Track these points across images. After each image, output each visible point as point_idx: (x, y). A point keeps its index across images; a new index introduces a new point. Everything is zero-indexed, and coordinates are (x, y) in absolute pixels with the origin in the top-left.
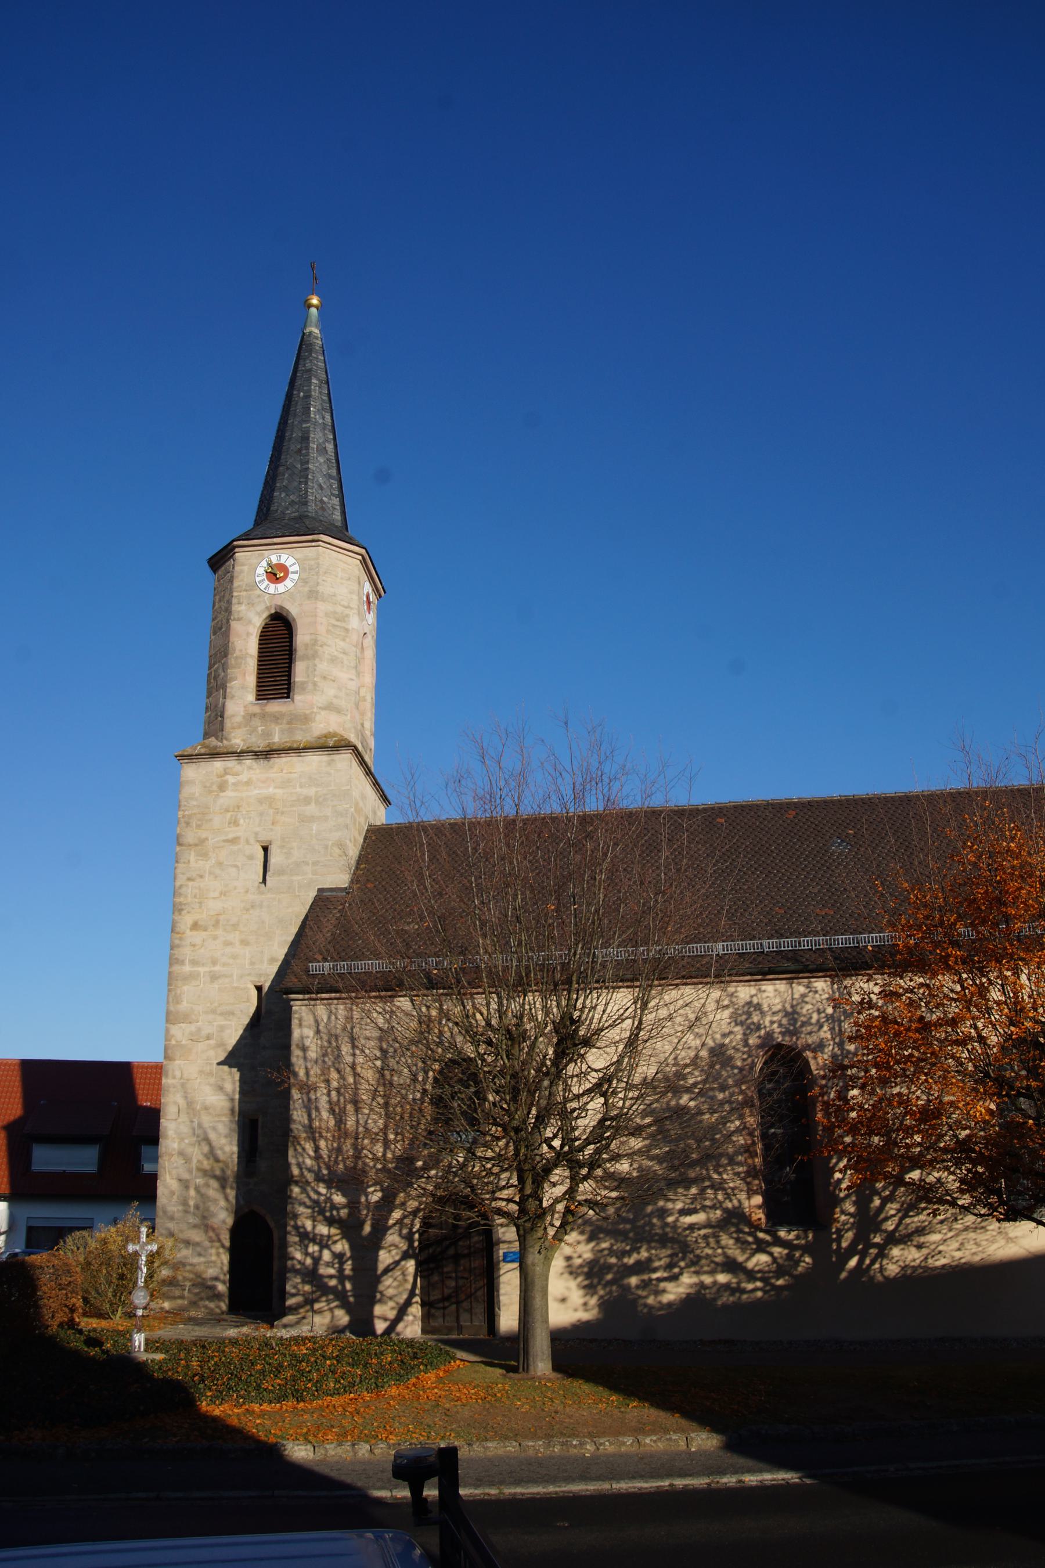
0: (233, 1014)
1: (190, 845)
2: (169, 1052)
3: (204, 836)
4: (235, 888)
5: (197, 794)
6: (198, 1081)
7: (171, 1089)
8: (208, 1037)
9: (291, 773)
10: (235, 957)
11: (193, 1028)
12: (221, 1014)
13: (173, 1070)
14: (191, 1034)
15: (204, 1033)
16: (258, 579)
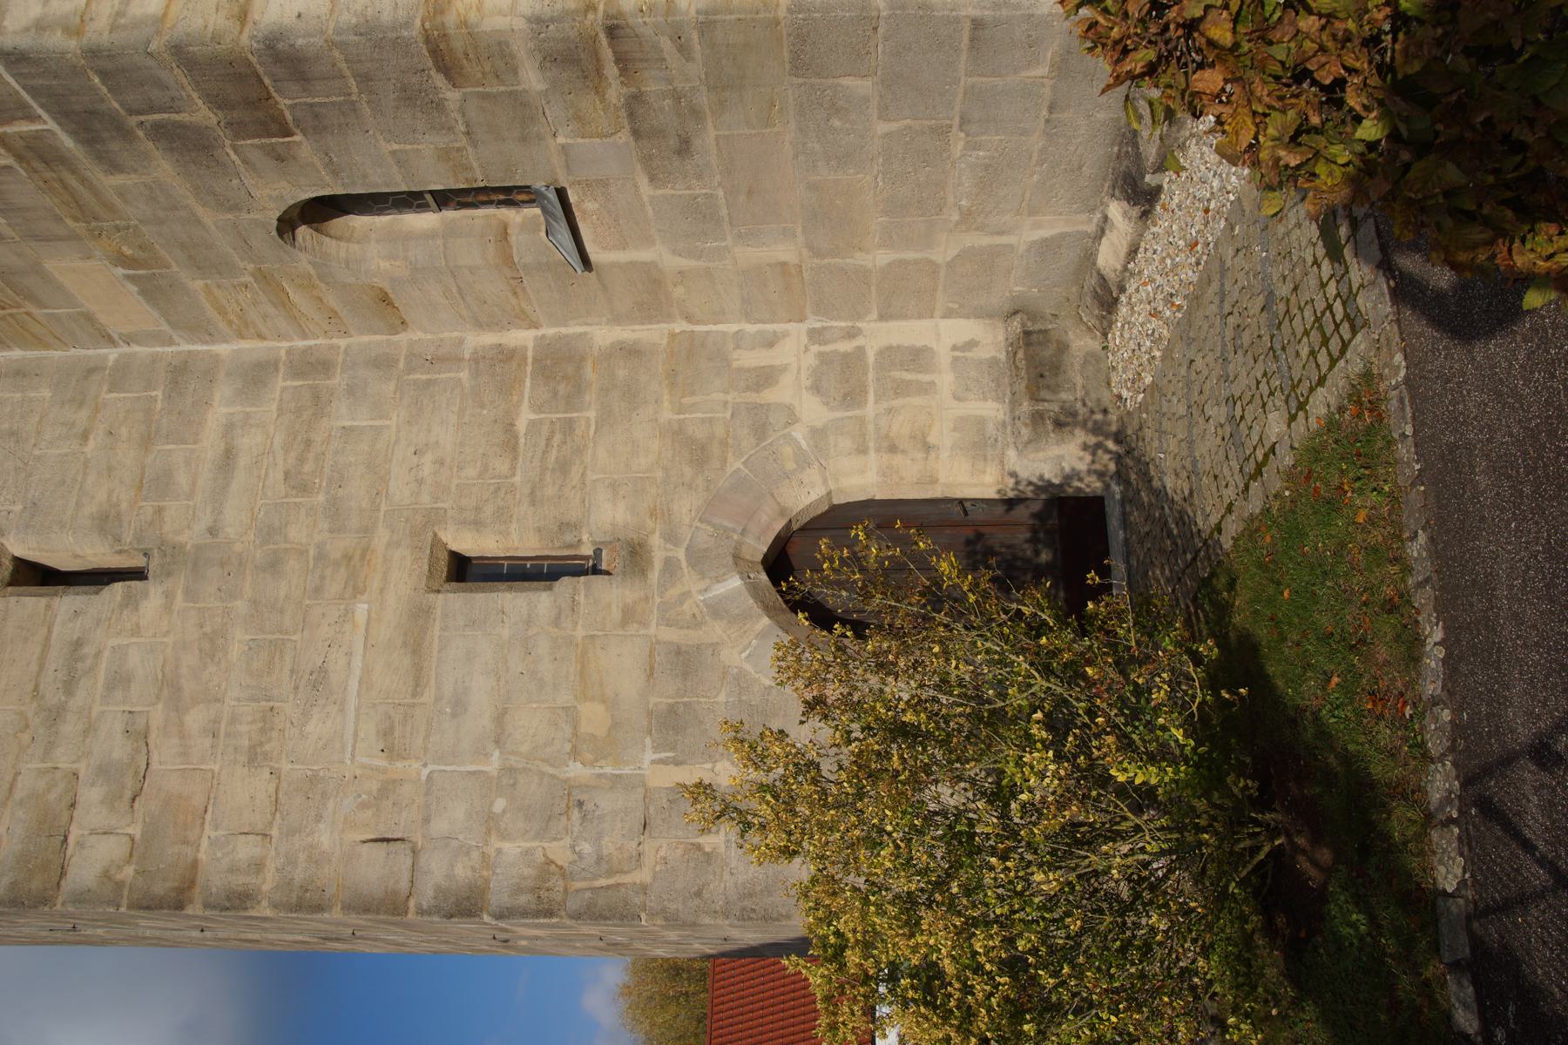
0: (78, 644)
2: (160, 888)
6: (286, 766)
7: (299, 875)
8: (139, 736)
11: (91, 795)
12: (69, 686)
13: (233, 870)
14: (110, 801)
15: (119, 749)
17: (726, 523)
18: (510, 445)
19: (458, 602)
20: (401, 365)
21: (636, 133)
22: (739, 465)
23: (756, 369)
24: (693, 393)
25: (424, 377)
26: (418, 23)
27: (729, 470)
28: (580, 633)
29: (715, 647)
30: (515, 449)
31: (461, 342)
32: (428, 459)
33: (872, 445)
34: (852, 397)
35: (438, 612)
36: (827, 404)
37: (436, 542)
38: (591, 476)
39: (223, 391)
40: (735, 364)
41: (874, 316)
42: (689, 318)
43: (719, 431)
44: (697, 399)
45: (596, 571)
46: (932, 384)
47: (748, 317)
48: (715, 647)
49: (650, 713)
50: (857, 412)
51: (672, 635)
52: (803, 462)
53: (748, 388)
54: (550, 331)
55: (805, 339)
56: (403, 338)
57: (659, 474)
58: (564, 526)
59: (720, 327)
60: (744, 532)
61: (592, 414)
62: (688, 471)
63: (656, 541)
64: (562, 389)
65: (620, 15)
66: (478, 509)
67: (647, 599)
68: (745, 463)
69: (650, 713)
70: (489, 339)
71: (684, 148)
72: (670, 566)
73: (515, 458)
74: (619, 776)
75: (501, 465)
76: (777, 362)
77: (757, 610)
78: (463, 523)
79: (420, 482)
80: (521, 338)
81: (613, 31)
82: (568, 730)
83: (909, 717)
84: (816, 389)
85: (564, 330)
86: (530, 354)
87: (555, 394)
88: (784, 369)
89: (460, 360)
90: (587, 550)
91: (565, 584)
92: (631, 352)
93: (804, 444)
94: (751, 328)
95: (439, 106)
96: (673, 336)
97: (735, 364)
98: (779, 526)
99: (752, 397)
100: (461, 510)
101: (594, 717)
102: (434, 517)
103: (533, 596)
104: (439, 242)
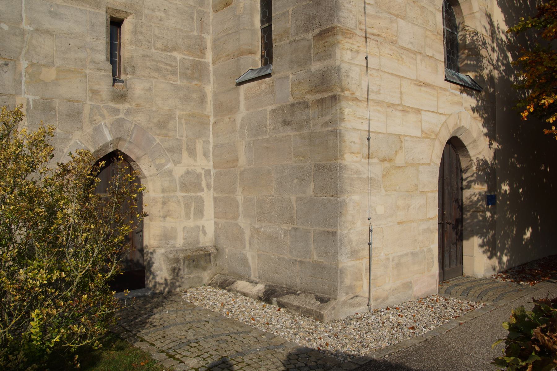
17: (134, 135)
18: (167, 49)
19: (102, 20)
20: (200, 8)
21: (293, 105)
22: (158, 141)
23: (195, 149)
24: (186, 123)
25: (195, 17)
26: (339, 25)
27: (156, 137)
28: (88, 71)
29: (81, 129)
30: (165, 50)
31: (208, 33)
32: (162, 14)
33: (166, 195)
34: (185, 187)
35: (97, 11)
36: (182, 177)
37: (128, 14)
38: (154, 81)
40: (197, 141)
41: (216, 195)
42: (215, 123)
43: (171, 134)
44: (184, 125)
45: (114, 80)
46: (190, 218)
47: (215, 146)
48: (81, 129)
49: (51, 99)
50: (178, 188)
51: (86, 110)
52: (159, 167)
53: (188, 146)
54: (211, 69)
55: (206, 168)
56: (210, 10)
57: (154, 109)
58: (134, 68)
59: (211, 136)
60: (130, 142)
61: (179, 83)
62: (155, 120)
63: (127, 106)
64: (189, 72)
65: (340, 101)
66: (141, 33)
67: (102, 101)
68: (158, 144)
69: (51, 99)
70: (209, 44)
71: (286, 123)
72: (116, 111)
73: (162, 50)
74: (21, 83)
75: (159, 45)
76: (198, 157)
77: (97, 147)
78: (136, 26)
79: (153, 10)
80: (209, 57)
81: (334, 98)
82: (43, 62)
83: (59, 215)
84: (188, 173)
85: (211, 74)
86: (203, 60)
87: (187, 69)
88: (195, 160)
89: (201, 32)
90: (123, 77)
91: (110, 67)
92: (202, 100)
93: (166, 167)
94: (211, 147)
95: (306, 30)
96: (208, 117)
97: (197, 141)
98: (132, 157)
99: (184, 147)
100: (141, 26)
101: (49, 74)
102: (138, 14)
103: (104, 52)
104: (250, 27)
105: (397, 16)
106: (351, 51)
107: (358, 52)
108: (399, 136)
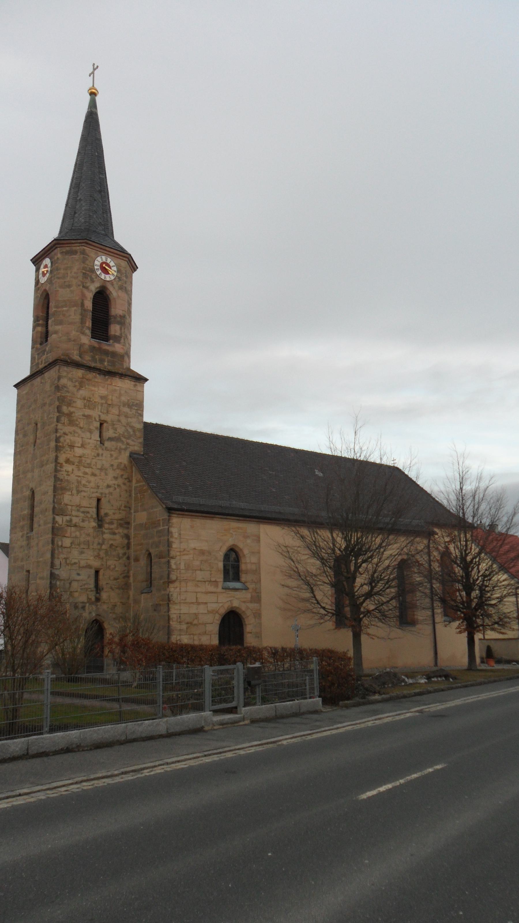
1: (65, 414)
3: (72, 410)
4: (89, 443)
5: (68, 385)
9: (116, 386)
10: (89, 482)
11: (68, 518)
16: (96, 267)
19: (93, 572)
39: (126, 531)
54: (132, 584)
71: (155, 610)
105: (196, 570)
106: (174, 587)
107: (177, 587)
108: (195, 614)
